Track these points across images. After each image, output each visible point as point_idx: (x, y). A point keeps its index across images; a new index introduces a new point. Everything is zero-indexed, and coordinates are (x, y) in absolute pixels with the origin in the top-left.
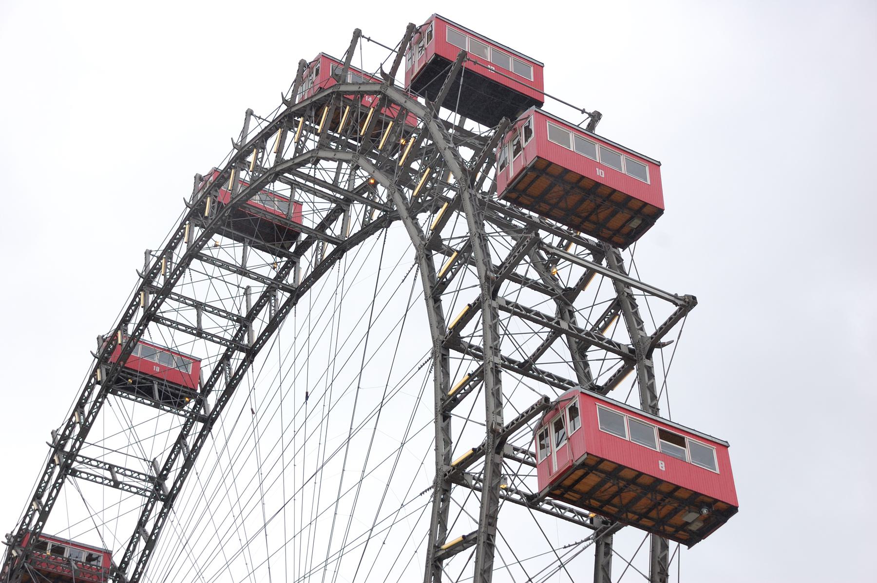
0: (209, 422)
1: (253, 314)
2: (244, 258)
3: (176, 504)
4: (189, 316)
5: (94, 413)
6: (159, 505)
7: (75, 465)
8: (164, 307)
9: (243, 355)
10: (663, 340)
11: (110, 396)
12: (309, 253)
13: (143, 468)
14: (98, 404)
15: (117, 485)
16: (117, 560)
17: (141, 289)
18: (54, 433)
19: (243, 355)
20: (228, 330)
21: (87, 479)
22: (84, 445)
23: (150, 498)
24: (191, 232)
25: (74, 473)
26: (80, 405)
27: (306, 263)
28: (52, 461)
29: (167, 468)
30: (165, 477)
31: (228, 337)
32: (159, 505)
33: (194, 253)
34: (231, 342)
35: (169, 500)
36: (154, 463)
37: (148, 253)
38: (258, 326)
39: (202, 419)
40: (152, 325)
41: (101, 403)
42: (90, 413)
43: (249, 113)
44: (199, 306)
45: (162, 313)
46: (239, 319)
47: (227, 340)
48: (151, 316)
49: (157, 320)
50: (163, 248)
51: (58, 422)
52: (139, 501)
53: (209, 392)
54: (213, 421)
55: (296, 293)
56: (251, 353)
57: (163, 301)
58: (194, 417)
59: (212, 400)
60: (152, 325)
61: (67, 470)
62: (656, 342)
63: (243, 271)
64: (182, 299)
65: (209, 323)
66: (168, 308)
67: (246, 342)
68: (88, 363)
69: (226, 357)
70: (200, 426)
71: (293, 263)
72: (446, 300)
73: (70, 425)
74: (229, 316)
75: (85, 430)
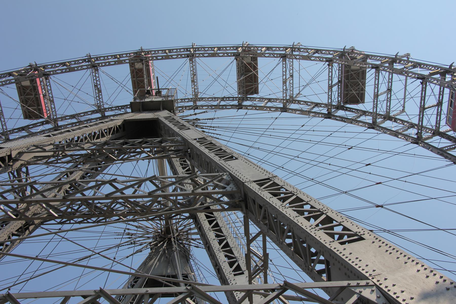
3: (284, 114)
4: (383, 88)
8: (384, 73)
9: (371, 122)
13: (296, 91)
17: (390, 58)
19: (371, 122)
22: (298, 60)
26: (317, 51)
28: (287, 48)
29: (299, 102)
31: (378, 110)
35: (284, 109)
38: (388, 124)
40: (374, 70)
42: (316, 57)
44: (389, 90)
45: (381, 72)
46: (388, 113)
52: (280, 95)
53: (343, 109)
56: (373, 126)
57: (386, 71)
58: (328, 106)
59: (341, 113)
61: (284, 57)
64: (390, 81)
66: (384, 75)
73: (306, 49)
74: (389, 108)
75: (304, 58)
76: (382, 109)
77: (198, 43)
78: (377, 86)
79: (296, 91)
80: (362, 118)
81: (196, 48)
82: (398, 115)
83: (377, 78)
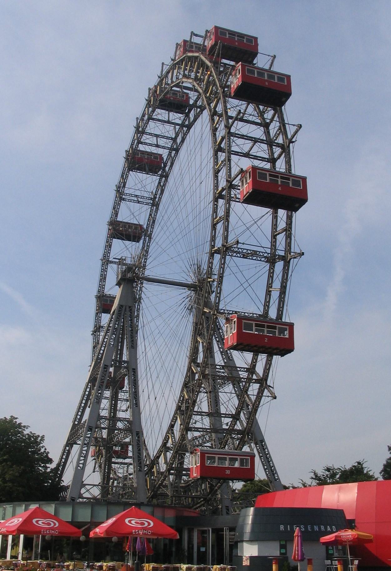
0: (167, 177)
4: (153, 140)
7: (123, 196)
10: (294, 140)
11: (130, 172)
12: (192, 112)
15: (139, 202)
16: (145, 227)
18: (116, 185)
20: (169, 144)
21: (128, 201)
24: (148, 110)
25: (124, 199)
27: (192, 115)
30: (156, 198)
36: (152, 192)
37: (137, 118)
38: (179, 140)
43: (163, 64)
44: (157, 136)
46: (172, 139)
50: (141, 116)
51: (116, 182)
54: (168, 177)
55: (189, 127)
56: (177, 150)
58: (161, 176)
59: (167, 169)
60: (140, 145)
61: (122, 199)
62: (291, 142)
64: (150, 134)
65: (161, 142)
67: (175, 147)
69: (170, 153)
70: (164, 179)
71: (187, 115)
72: (217, 133)
74: (167, 138)
76: (169, 144)
77: (101, 256)
78: (151, 145)
80: (173, 155)
81: (103, 258)
82: (175, 131)
83: (146, 144)
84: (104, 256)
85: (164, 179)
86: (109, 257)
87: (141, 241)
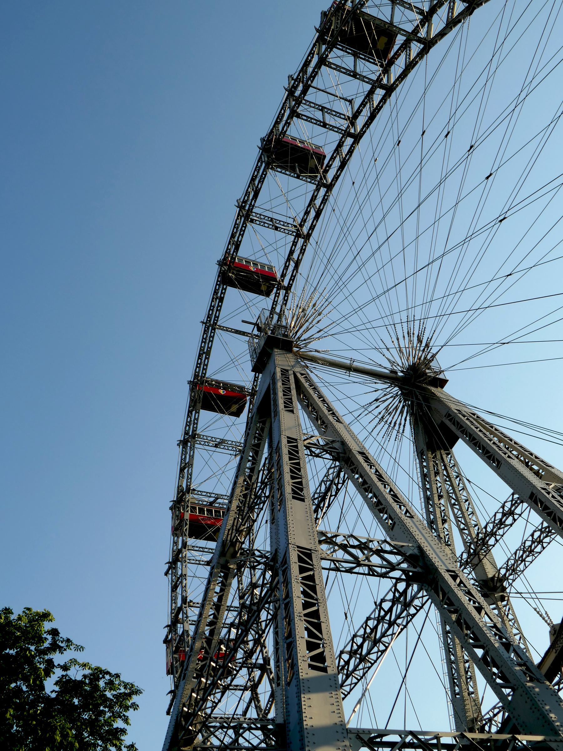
0: (330, 187)
1: (356, 115)
2: (355, 66)
5: (262, 181)
6: (301, 241)
9: (352, 140)
14: (263, 176)
15: (276, 228)
16: (278, 276)
19: (352, 140)
23: (296, 237)
27: (397, 70)
29: (304, 221)
32: (301, 241)
33: (323, 61)
34: (345, 131)
38: (361, 122)
39: (325, 186)
40: (295, 118)
41: (265, 175)
42: (259, 182)
44: (322, 109)
47: (342, 130)
48: (294, 114)
49: (299, 116)
51: (239, 194)
55: (390, 90)
58: (319, 186)
60: (295, 118)
63: (354, 75)
68: (255, 153)
71: (386, 70)
73: (247, 193)
77: (203, 316)
79: (290, 221)
80: (345, 149)
81: (207, 320)
84: (208, 317)
85: (323, 191)
86: (218, 317)
87: (272, 296)
